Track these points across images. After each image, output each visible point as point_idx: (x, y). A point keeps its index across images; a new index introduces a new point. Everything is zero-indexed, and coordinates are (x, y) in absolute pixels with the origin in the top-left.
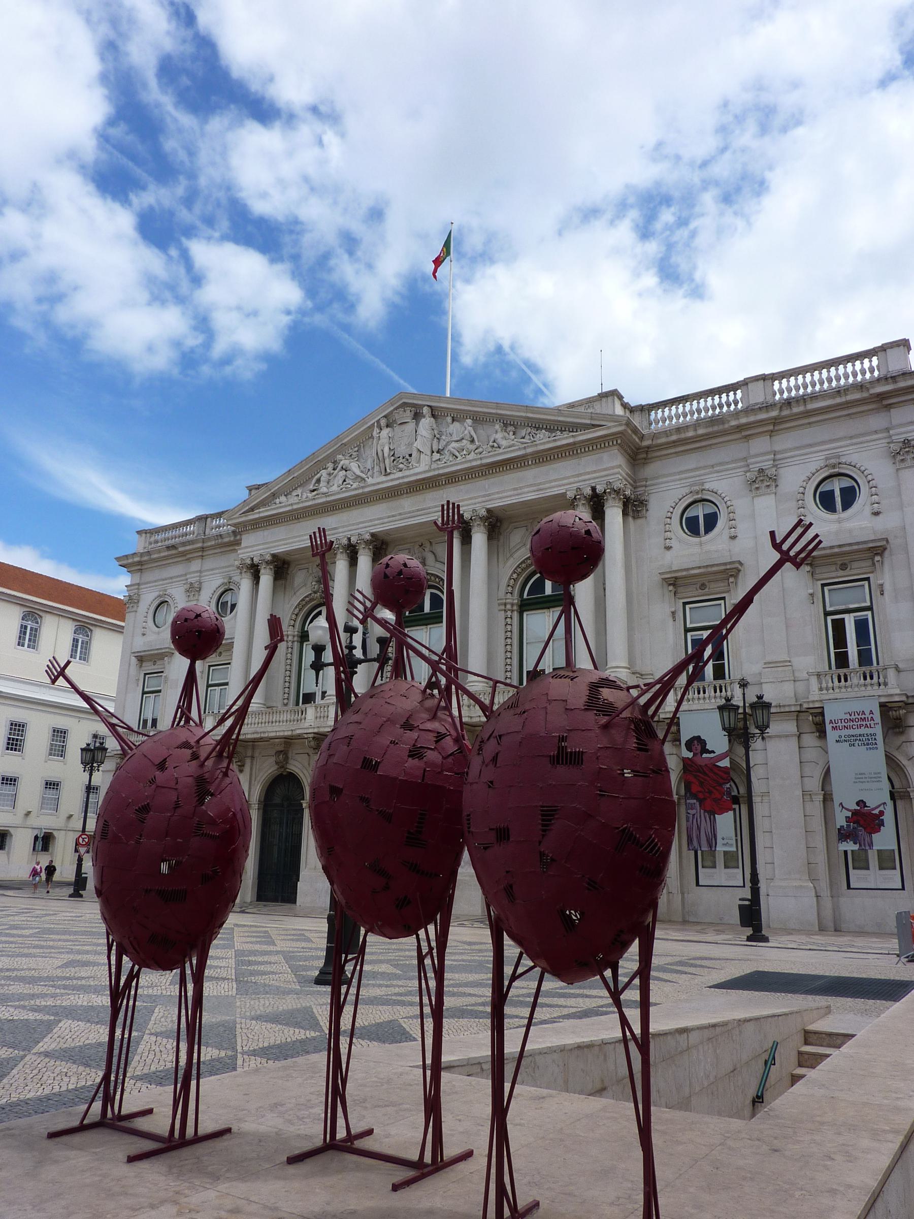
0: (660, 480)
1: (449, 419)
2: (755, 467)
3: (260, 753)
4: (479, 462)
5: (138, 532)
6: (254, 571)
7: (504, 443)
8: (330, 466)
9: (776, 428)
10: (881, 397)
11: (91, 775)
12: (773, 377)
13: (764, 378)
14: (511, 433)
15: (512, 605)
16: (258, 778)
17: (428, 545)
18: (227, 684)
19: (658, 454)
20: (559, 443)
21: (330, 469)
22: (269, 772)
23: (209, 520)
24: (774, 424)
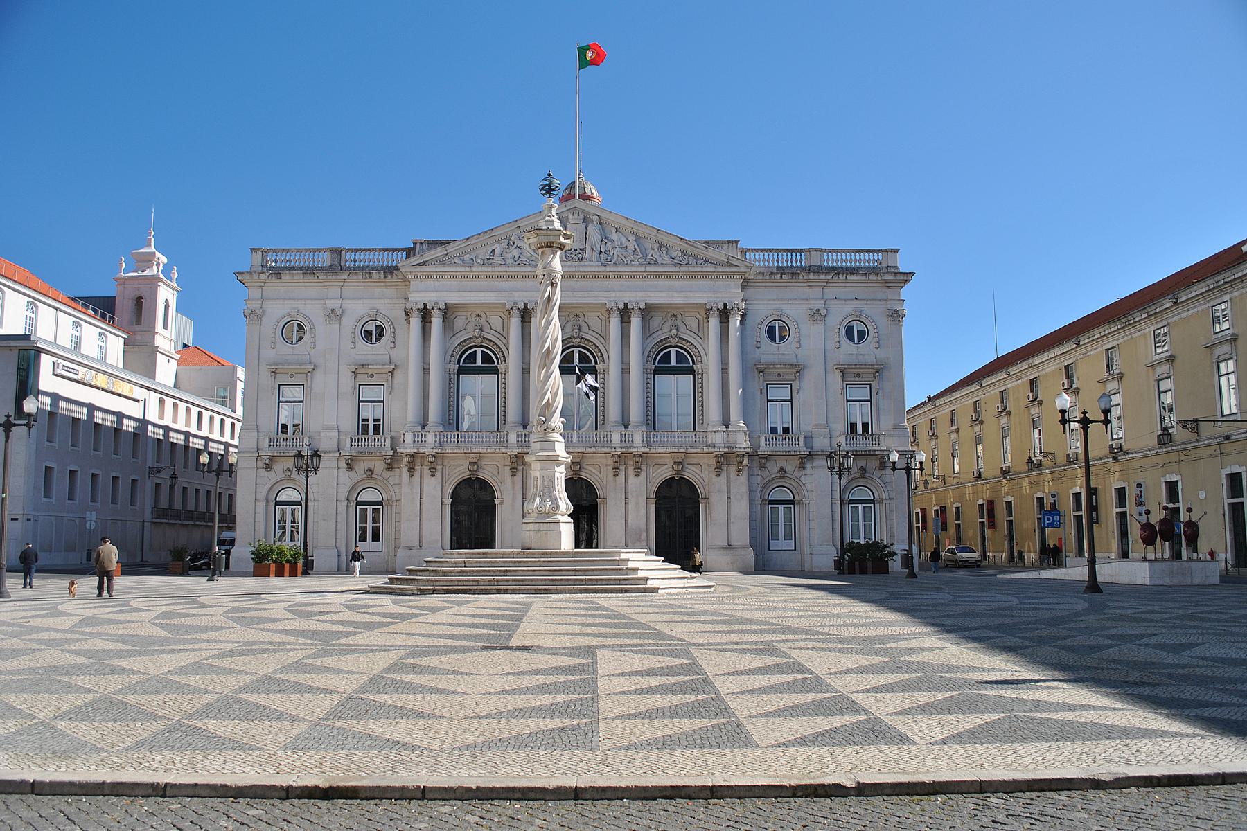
0: (754, 302)
1: (614, 230)
2: (817, 307)
3: (448, 463)
4: (643, 269)
5: (251, 249)
6: (426, 314)
7: (660, 260)
8: (507, 241)
9: (828, 285)
10: (886, 281)
11: (307, 478)
12: (825, 251)
13: (820, 251)
14: (664, 253)
15: (650, 370)
16: (449, 482)
17: (581, 315)
18: (383, 402)
19: (752, 284)
20: (705, 269)
21: (504, 245)
22: (460, 477)
23: (343, 253)
24: (827, 283)
